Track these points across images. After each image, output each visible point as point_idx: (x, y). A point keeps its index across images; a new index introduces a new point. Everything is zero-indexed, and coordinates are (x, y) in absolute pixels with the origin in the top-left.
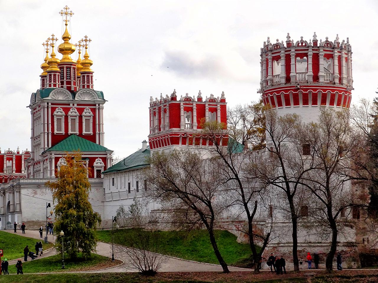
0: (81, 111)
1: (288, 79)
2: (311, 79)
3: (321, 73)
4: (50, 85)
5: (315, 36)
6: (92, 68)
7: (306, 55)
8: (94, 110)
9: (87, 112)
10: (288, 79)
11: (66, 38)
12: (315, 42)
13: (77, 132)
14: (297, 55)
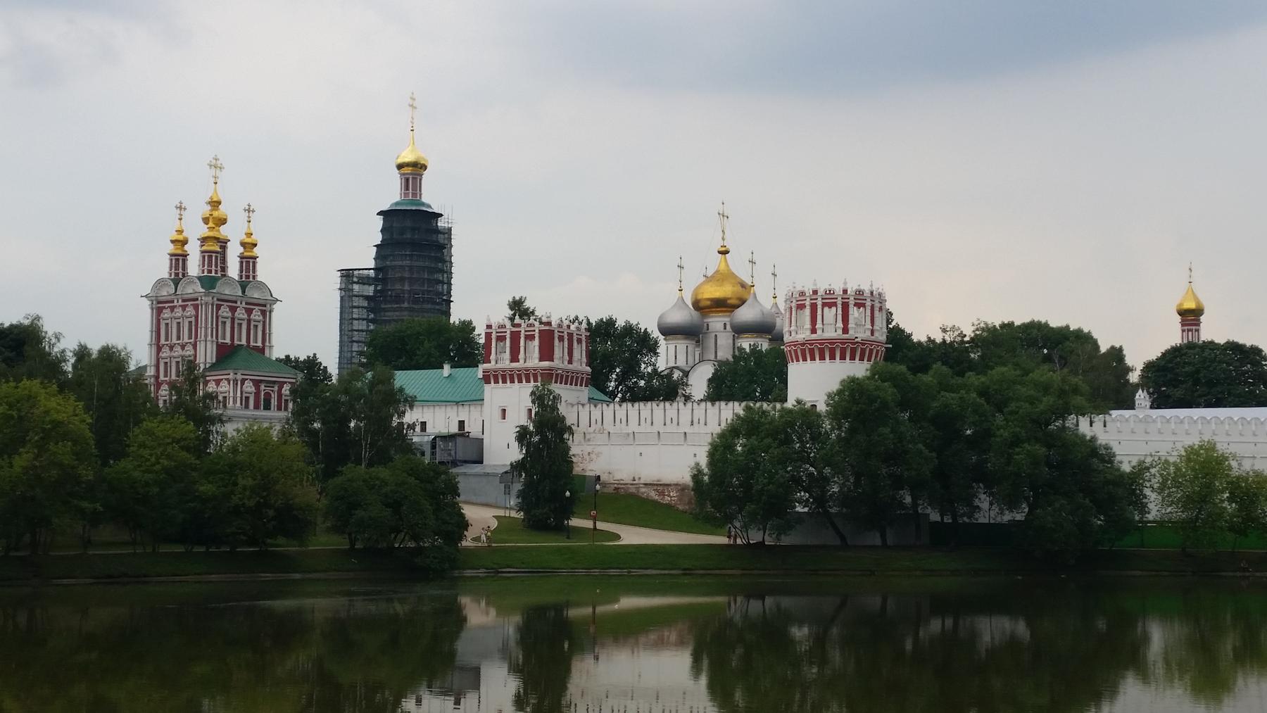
0: (249, 312)
1: (814, 331)
2: (840, 331)
3: (851, 325)
4: (210, 271)
5: (845, 283)
6: (256, 251)
7: (835, 304)
8: (263, 313)
9: (256, 315)
10: (814, 331)
11: (215, 204)
12: (845, 291)
13: (244, 342)
14: (824, 305)
